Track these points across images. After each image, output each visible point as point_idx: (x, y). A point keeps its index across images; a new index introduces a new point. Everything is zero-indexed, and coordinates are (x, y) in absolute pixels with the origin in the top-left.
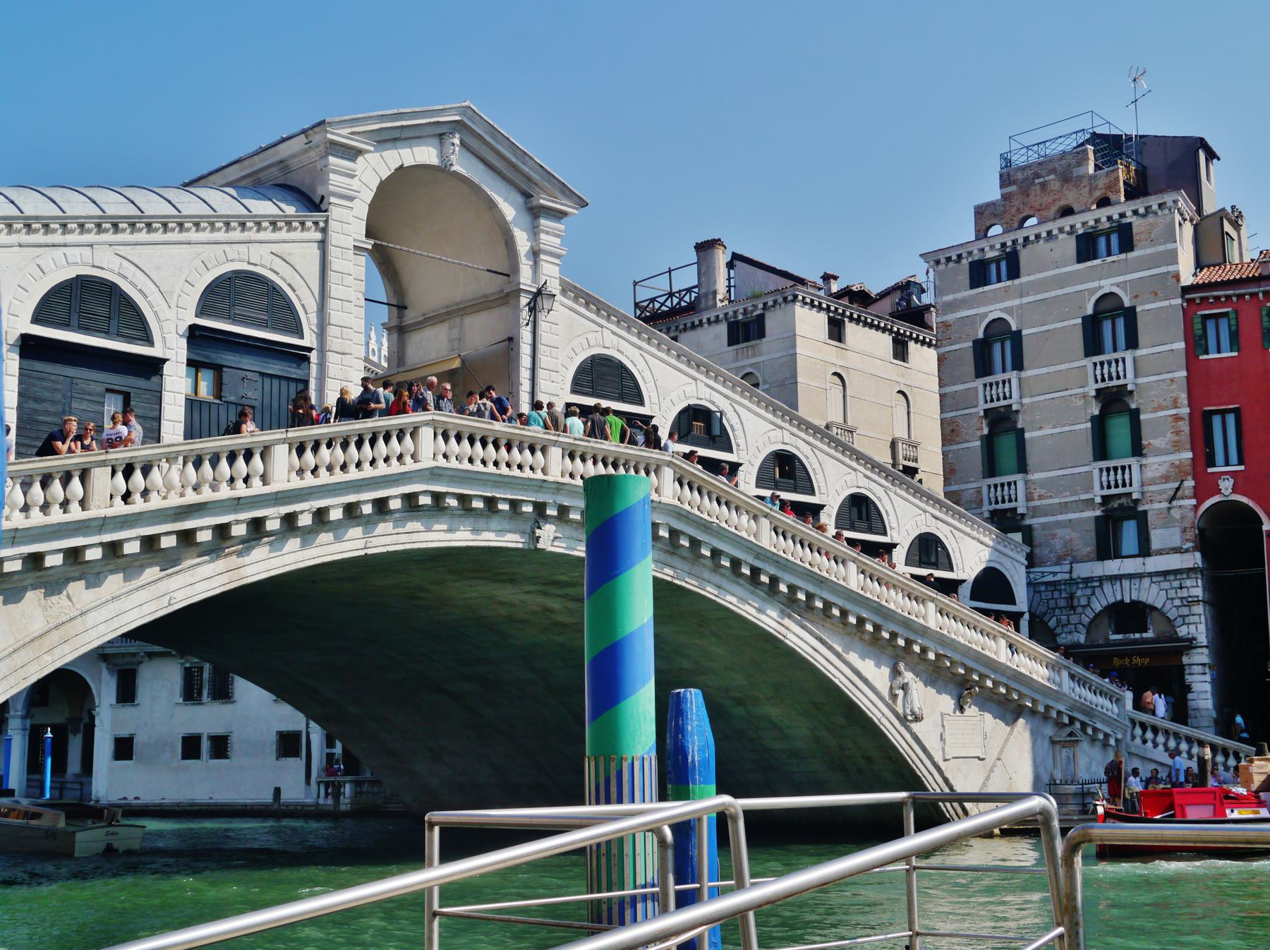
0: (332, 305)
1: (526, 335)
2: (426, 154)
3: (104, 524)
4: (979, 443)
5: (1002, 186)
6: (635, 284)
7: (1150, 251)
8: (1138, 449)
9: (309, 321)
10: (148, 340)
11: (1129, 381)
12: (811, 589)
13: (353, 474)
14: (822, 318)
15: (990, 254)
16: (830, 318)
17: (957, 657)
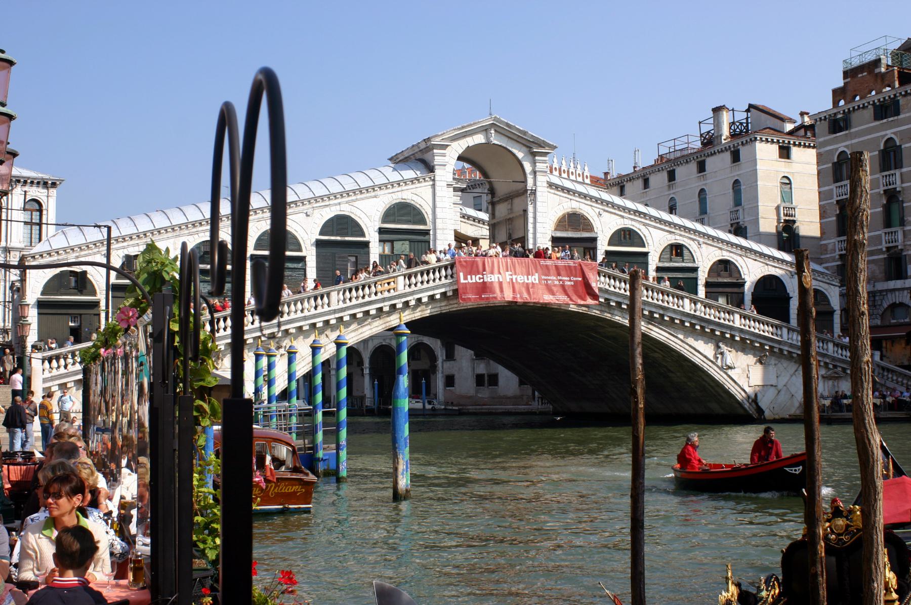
0: (437, 210)
1: (530, 209)
2: (479, 139)
3: (335, 311)
4: (834, 218)
5: (845, 78)
6: (700, 123)
7: (908, 115)
8: (902, 223)
9: (429, 218)
10: (363, 235)
11: (898, 185)
12: (661, 312)
13: (431, 284)
14: (777, 147)
15: (839, 116)
16: (780, 147)
17: (752, 338)
